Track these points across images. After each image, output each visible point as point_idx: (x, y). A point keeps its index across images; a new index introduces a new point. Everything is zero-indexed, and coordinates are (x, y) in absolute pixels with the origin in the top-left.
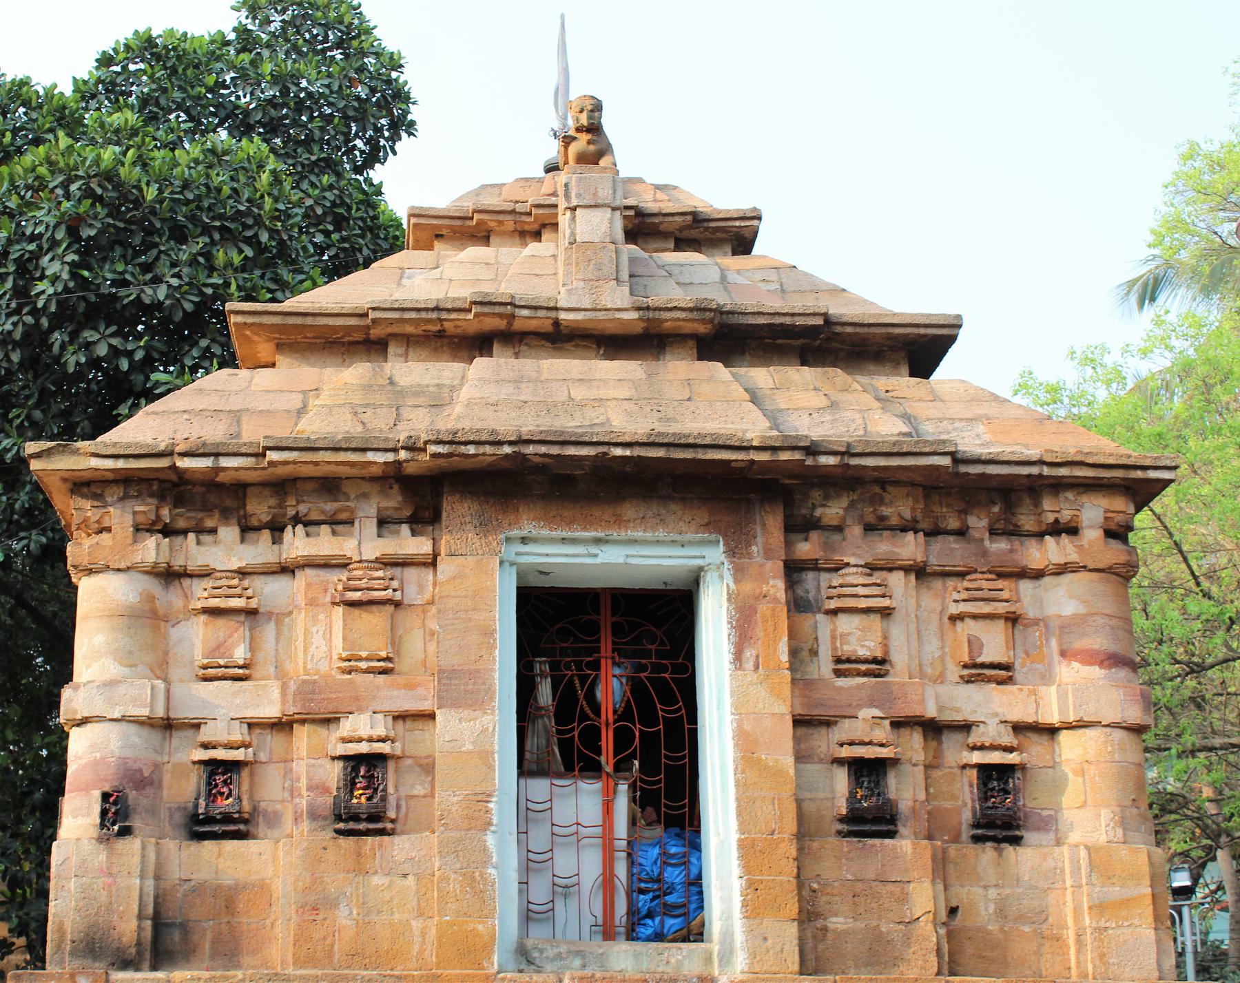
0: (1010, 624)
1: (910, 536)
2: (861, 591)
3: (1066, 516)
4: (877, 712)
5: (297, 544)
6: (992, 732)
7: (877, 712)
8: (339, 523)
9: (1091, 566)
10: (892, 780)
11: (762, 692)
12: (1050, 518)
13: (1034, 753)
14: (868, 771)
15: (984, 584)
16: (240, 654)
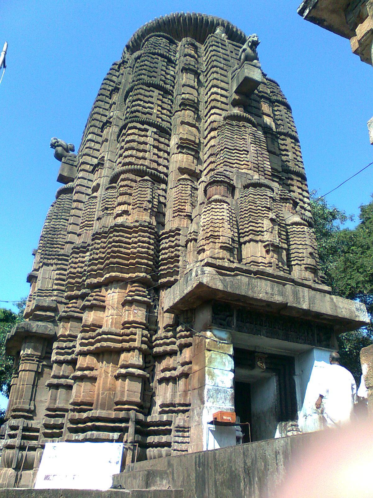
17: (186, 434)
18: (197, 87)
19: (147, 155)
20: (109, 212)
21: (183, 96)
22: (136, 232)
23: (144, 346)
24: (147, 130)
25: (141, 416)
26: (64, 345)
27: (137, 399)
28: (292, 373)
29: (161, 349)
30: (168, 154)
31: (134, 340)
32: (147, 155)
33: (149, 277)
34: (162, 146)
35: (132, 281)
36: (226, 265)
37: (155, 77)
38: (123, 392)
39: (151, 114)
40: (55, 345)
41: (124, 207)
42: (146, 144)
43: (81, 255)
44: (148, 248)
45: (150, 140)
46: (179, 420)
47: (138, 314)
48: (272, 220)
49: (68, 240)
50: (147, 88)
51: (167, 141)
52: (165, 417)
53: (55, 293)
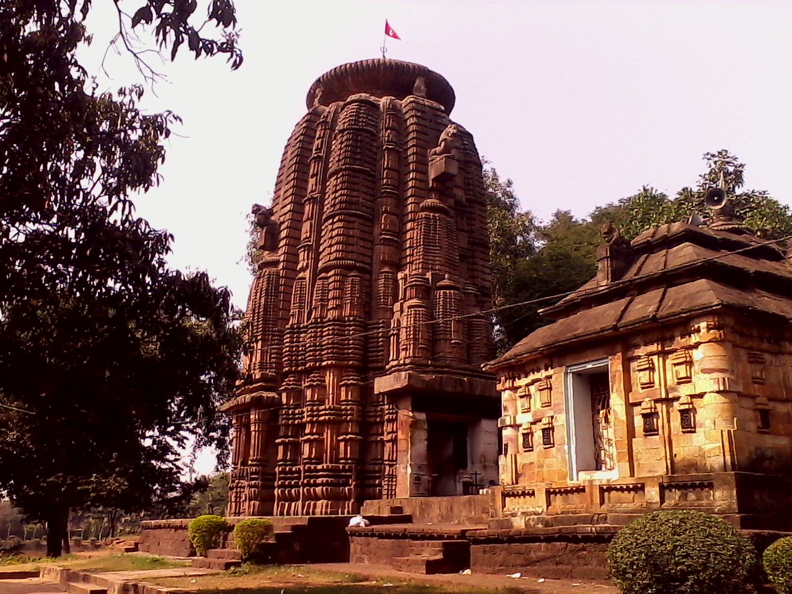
2: (643, 363)
4: (649, 399)
5: (532, 377)
8: (538, 371)
11: (618, 399)
23: (360, 419)
30: (372, 242)
34: (367, 236)
39: (357, 204)
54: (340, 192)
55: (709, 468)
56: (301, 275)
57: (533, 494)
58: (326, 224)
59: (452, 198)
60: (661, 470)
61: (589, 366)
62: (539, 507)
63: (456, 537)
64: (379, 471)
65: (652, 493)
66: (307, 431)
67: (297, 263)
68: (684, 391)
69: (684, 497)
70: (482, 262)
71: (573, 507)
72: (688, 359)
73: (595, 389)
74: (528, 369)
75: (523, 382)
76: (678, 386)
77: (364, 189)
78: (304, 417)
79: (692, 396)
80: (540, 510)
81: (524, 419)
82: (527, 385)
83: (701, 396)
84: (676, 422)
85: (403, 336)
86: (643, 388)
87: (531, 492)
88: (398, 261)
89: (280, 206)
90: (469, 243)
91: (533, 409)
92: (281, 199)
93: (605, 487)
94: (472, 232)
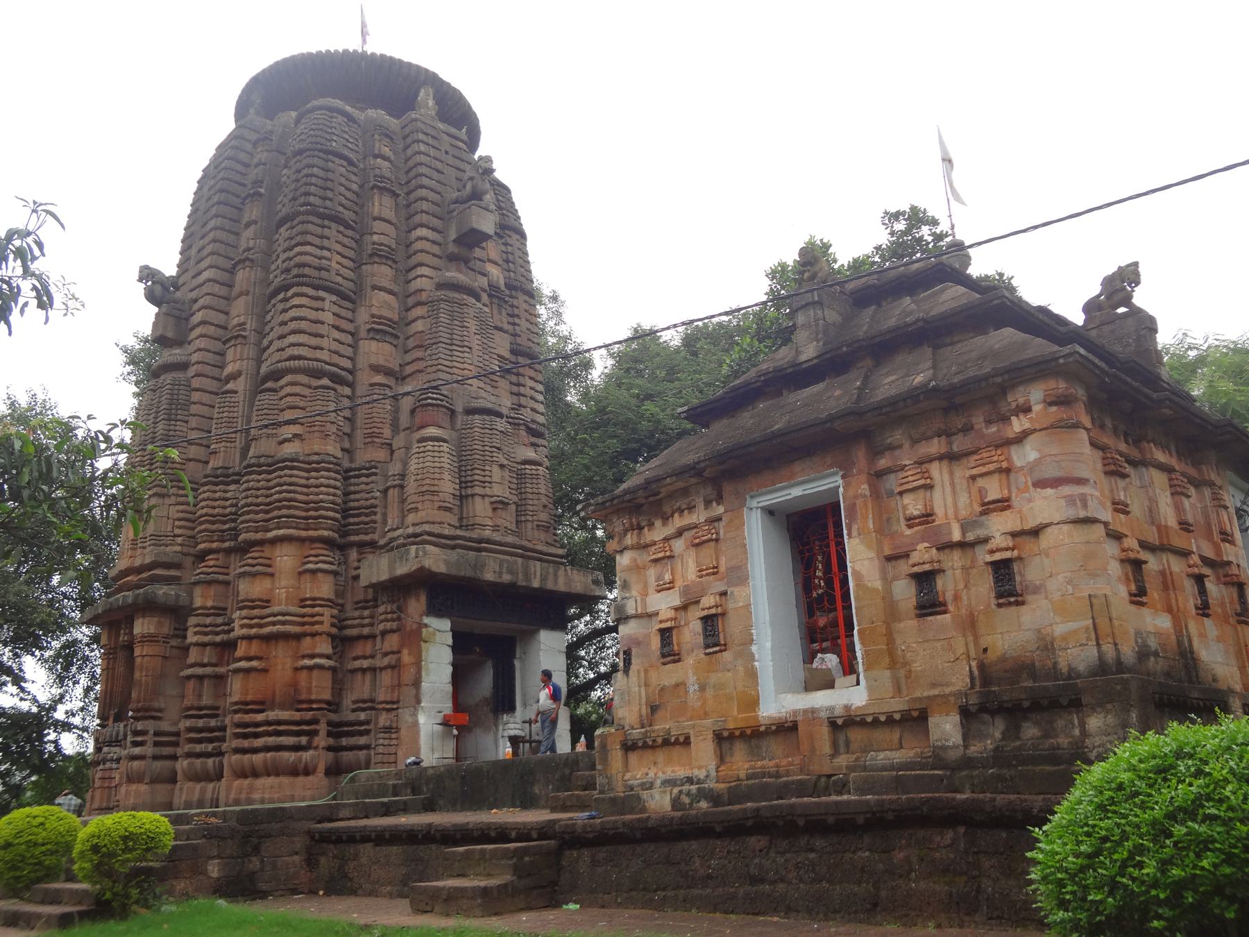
0: (1004, 476)
1: (936, 440)
2: (910, 479)
3: (1021, 401)
4: (926, 545)
5: (678, 522)
6: (999, 541)
7: (926, 545)
8: (691, 508)
9: (1038, 427)
10: (940, 582)
12: (1014, 405)
13: (1029, 545)
14: (924, 579)
15: (985, 455)
16: (667, 577)
17: (394, 736)
18: (394, 221)
19: (324, 342)
20: (270, 431)
21: (375, 238)
22: (317, 470)
23: (334, 631)
24: (323, 299)
25: (334, 717)
26: (208, 620)
27: (327, 695)
28: (512, 656)
29: (354, 632)
31: (321, 623)
32: (324, 342)
33: (336, 535)
35: (313, 540)
36: (446, 532)
37: (331, 200)
38: (309, 690)
40: (192, 621)
41: (296, 429)
42: (323, 323)
43: (222, 487)
44: (334, 495)
45: (328, 317)
46: (384, 720)
47: (325, 588)
48: (502, 466)
49: (191, 456)
50: (319, 221)
51: (349, 315)
52: (362, 716)
53: (179, 540)
54: (298, 249)
55: (1065, 670)
56: (230, 386)
57: (687, 742)
58: (273, 301)
59: (485, 275)
60: (959, 680)
61: (796, 492)
62: (700, 768)
63: (535, 835)
64: (368, 722)
65: (946, 728)
66: (240, 652)
67: (222, 367)
68: (999, 527)
69: (1013, 731)
70: (531, 383)
71: (771, 764)
72: (1005, 465)
73: (812, 537)
74: (667, 508)
75: (658, 532)
76: (984, 518)
77: (339, 248)
78: (233, 630)
79: (1014, 535)
80: (702, 774)
81: (664, 604)
82: (666, 539)
83: (1036, 532)
84: (984, 586)
85: (411, 487)
86: (910, 527)
87: (682, 739)
88: (397, 369)
89: (191, 273)
90: (513, 352)
91: (679, 583)
92: (192, 262)
93: (840, 722)
94: (515, 335)
